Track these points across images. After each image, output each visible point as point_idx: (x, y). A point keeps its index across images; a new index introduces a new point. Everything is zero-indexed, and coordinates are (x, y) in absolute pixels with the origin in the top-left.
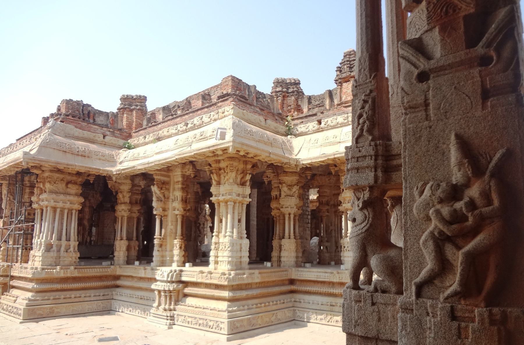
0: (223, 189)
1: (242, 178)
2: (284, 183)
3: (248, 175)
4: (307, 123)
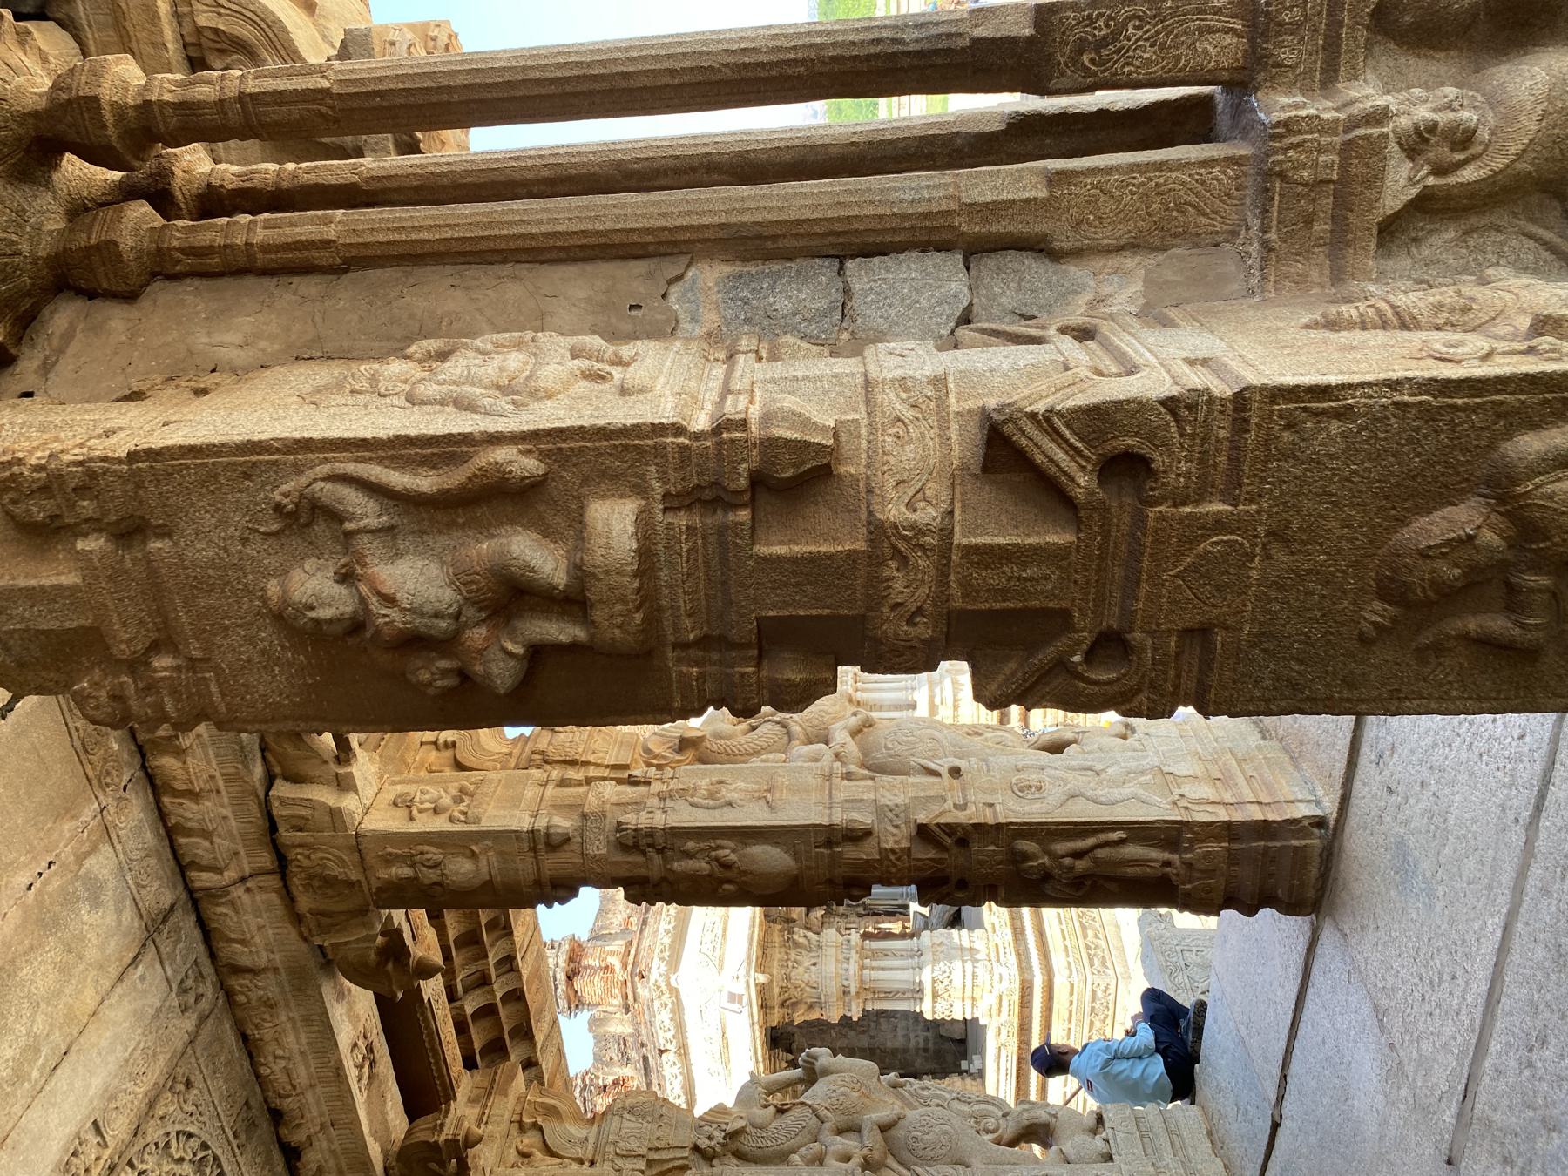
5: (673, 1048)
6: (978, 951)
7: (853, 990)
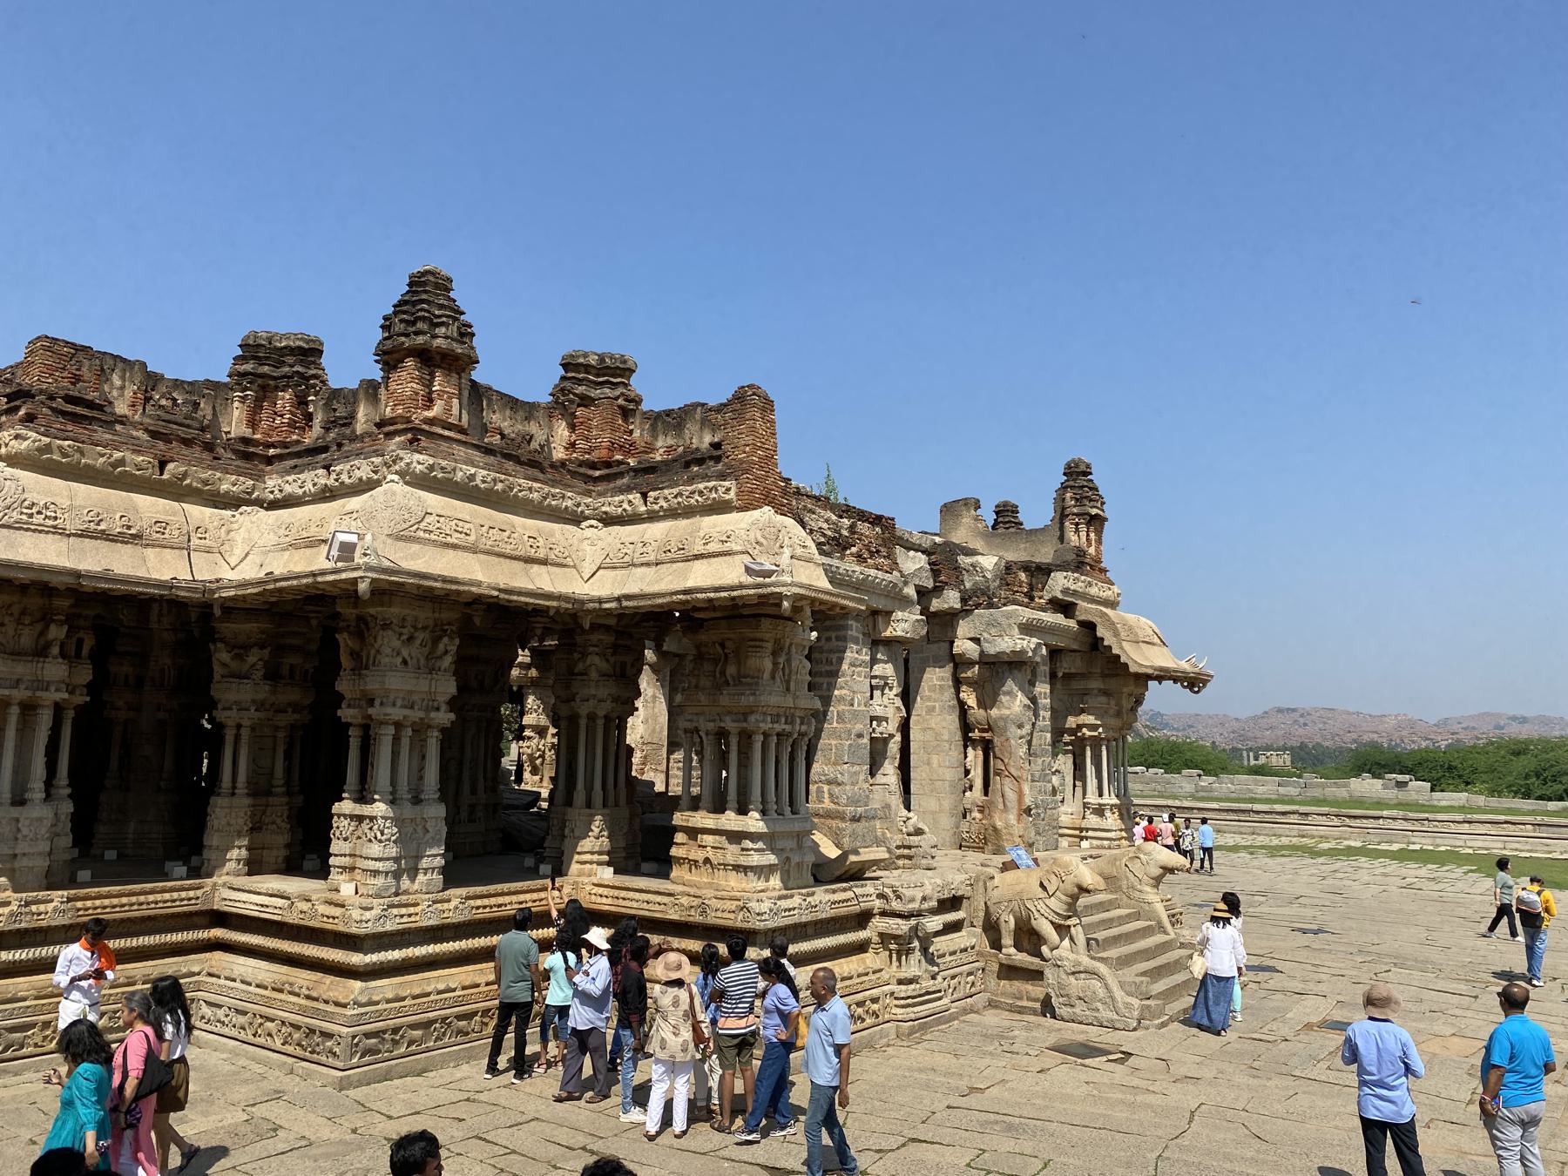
1: (42, 633)
2: (222, 640)
3: (53, 628)
5: (331, 482)
6: (413, 879)
7: (370, 711)
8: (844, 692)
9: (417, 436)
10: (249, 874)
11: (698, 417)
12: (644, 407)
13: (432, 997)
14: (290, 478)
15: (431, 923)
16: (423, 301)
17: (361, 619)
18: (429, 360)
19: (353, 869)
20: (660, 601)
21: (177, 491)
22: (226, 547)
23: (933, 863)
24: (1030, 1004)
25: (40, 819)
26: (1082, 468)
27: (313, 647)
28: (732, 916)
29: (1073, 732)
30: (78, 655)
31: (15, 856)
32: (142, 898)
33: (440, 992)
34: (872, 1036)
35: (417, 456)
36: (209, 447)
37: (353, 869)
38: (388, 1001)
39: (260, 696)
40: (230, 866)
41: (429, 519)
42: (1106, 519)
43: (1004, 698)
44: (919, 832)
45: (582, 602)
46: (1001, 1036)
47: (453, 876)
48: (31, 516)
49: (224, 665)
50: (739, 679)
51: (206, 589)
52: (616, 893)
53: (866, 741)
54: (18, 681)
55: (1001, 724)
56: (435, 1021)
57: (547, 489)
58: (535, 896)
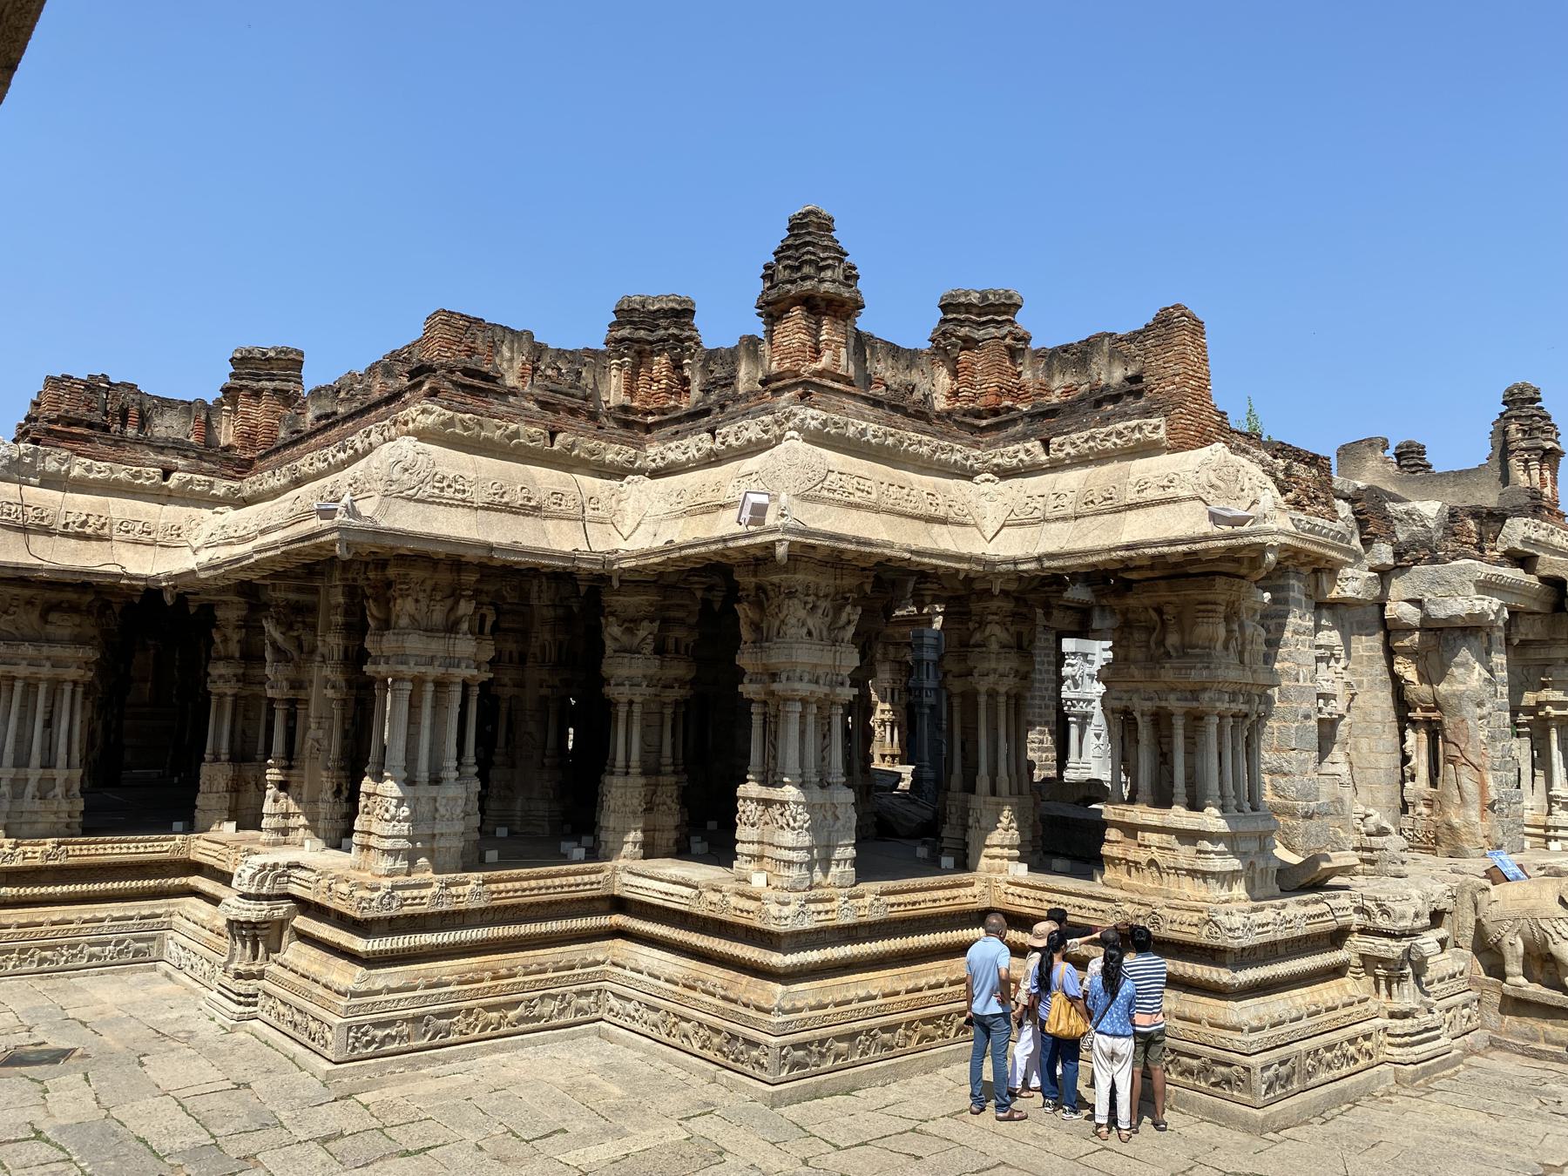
0: (389, 643)
1: (452, 609)
2: (612, 614)
3: (462, 603)
4: (685, 437)
5: (717, 446)
7: (775, 686)
8: (1287, 665)
9: (808, 389)
10: (645, 857)
11: (1106, 348)
12: (1034, 345)
13: (854, 1006)
14: (673, 445)
15: (848, 921)
16: (807, 244)
17: (760, 588)
18: (819, 307)
19: (761, 857)
20: (1095, 559)
21: (565, 462)
22: (618, 517)
23: (1405, 869)
24: (1550, 1048)
25: (455, 799)
26: (1530, 394)
27: (693, 620)
28: (1194, 930)
29: (1531, 710)
30: (481, 632)
31: (434, 836)
32: (549, 882)
33: (861, 1000)
34: (1369, 1080)
35: (810, 411)
36: (593, 416)
37: (761, 857)
38: (812, 1008)
39: (650, 672)
40: (628, 848)
41: (832, 477)
42: (1562, 454)
43: (1456, 671)
44: (1382, 832)
45: (993, 564)
46: (1534, 1089)
47: (865, 870)
48: (442, 490)
49: (616, 639)
50: (1184, 650)
51: (607, 560)
52: (1039, 894)
53: (1313, 723)
54: (433, 658)
55: (1454, 701)
56: (860, 1033)
57: (936, 442)
58: (948, 893)
